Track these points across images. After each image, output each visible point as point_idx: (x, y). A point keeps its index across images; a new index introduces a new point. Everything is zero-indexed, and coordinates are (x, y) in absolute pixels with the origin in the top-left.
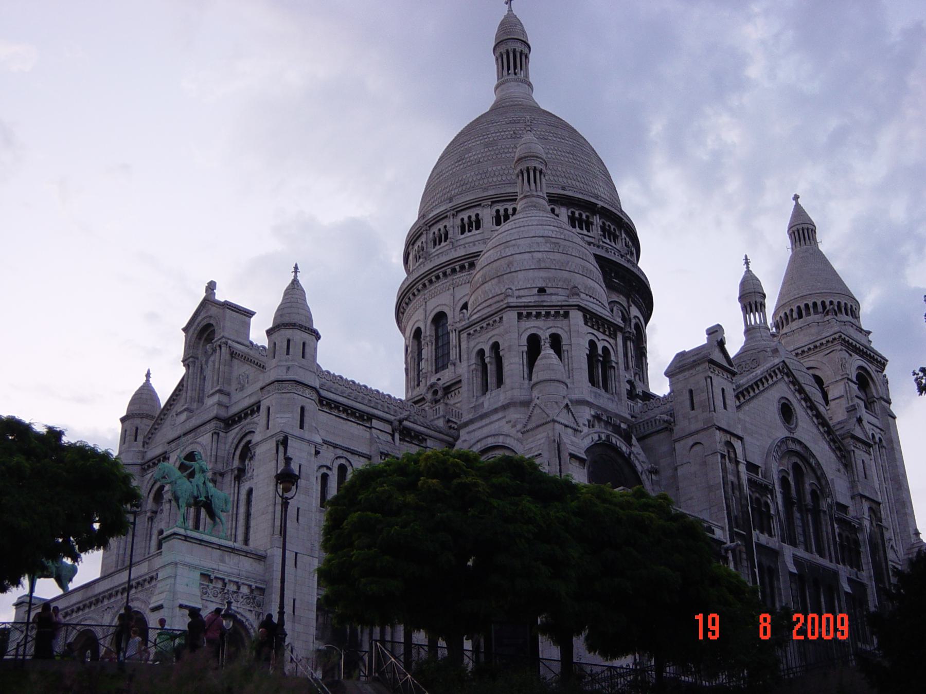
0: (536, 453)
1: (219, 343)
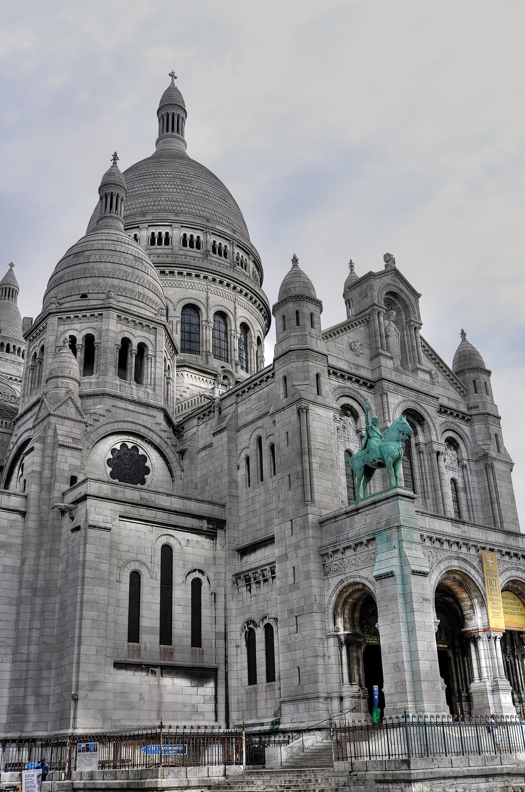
1: (417, 325)
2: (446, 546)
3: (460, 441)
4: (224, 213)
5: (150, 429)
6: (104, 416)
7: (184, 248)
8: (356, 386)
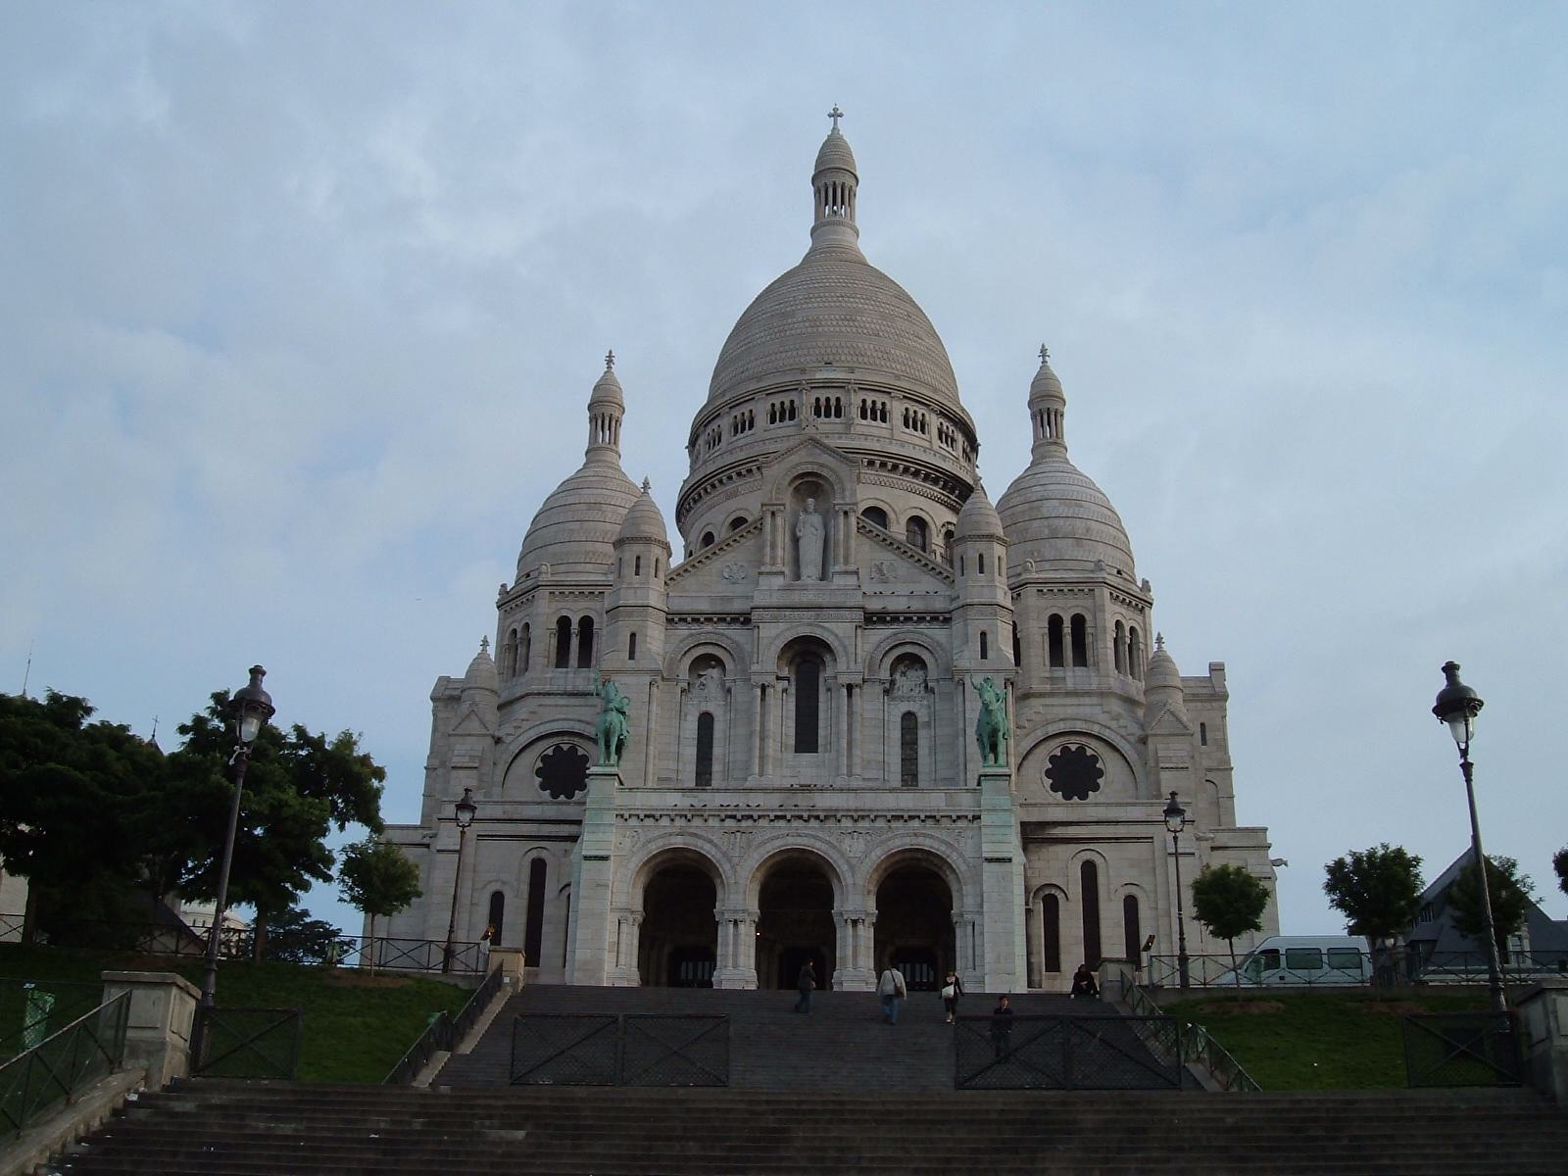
1: (847, 508)
2: (665, 822)
3: (925, 656)
4: (843, 344)
5: (588, 723)
6: (527, 720)
8: (722, 626)
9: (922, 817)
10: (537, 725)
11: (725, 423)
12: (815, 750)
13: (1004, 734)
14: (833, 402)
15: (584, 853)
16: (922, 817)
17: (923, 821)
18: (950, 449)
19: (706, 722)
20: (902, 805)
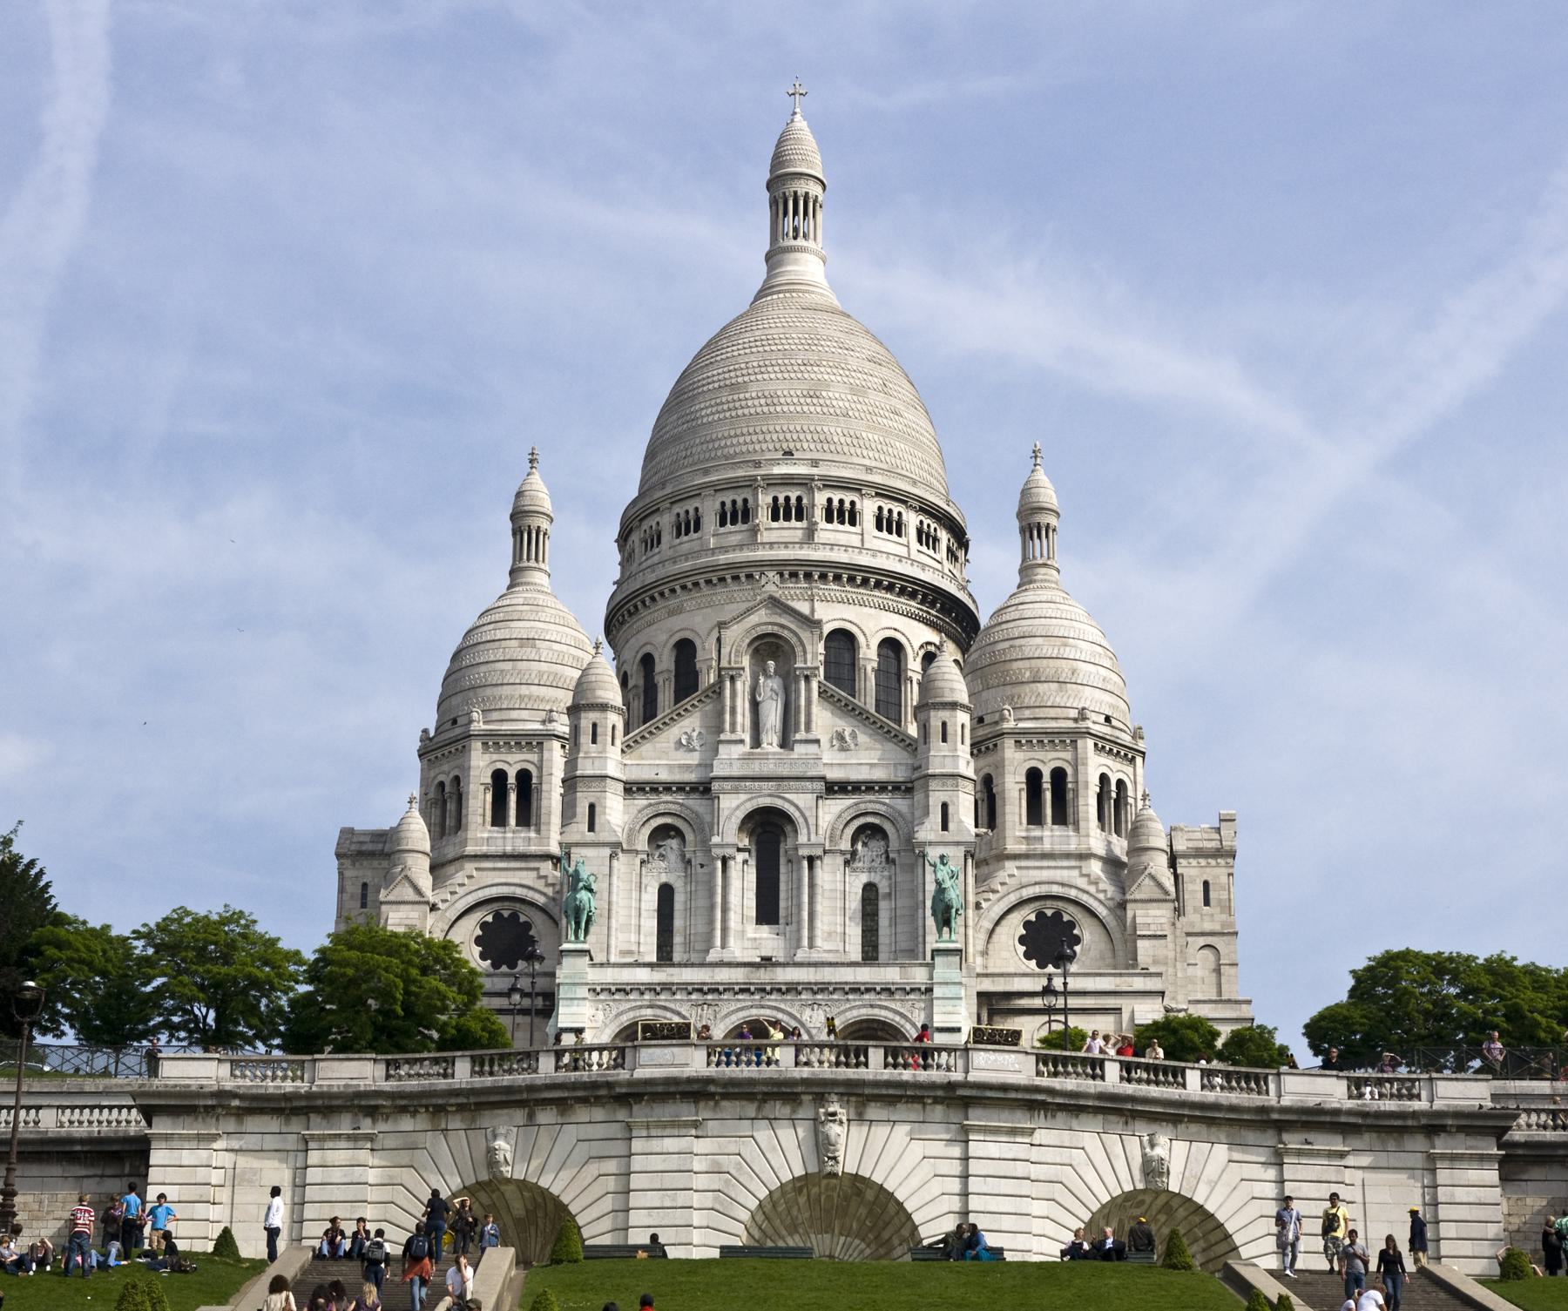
0: (1159, 933)
1: (808, 673)
3: (887, 826)
4: (805, 428)
5: (529, 888)
6: (464, 885)
7: (722, 530)
8: (680, 798)
9: (878, 988)
10: (476, 890)
11: (666, 521)
12: (778, 924)
13: (957, 910)
14: (793, 501)
15: (560, 1025)
16: (878, 988)
17: (879, 993)
18: (931, 552)
19: (666, 893)
20: (860, 979)
